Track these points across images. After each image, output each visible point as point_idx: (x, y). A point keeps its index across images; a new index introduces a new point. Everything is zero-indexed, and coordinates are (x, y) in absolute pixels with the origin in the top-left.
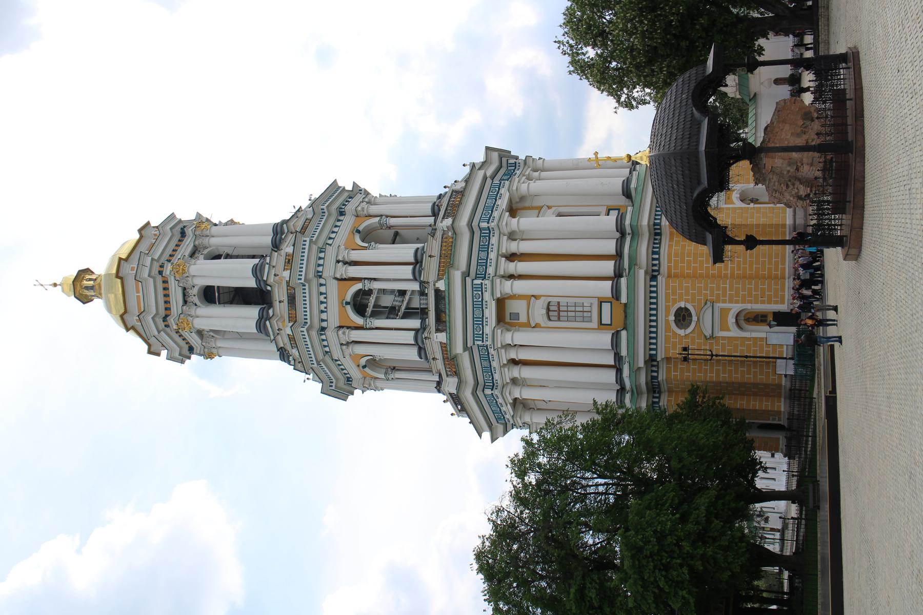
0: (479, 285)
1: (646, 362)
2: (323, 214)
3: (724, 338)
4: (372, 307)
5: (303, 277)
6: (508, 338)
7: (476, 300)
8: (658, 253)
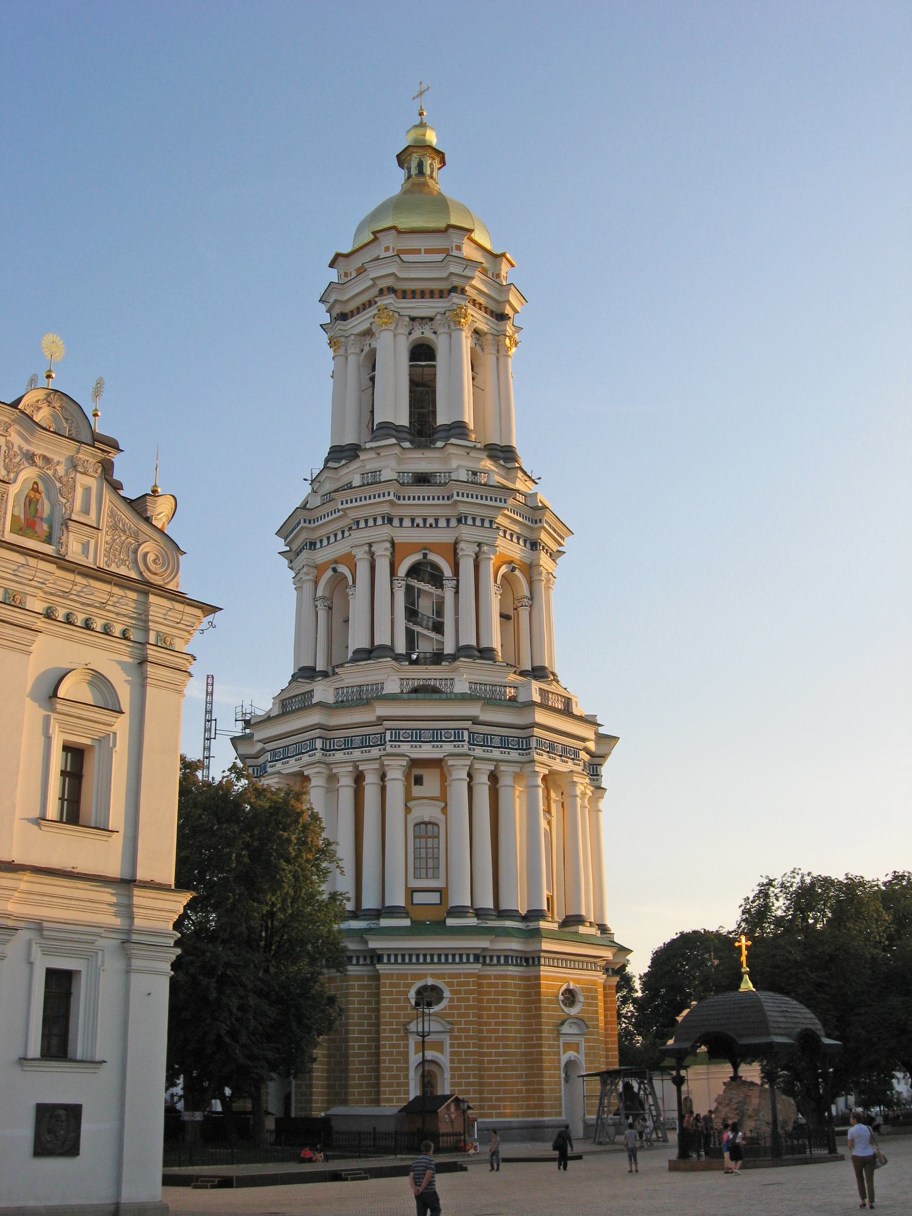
0: (462, 738)
1: (374, 950)
2: (534, 521)
3: (406, 1046)
4: (420, 586)
5: (460, 498)
6: (396, 775)
7: (443, 733)
8: (506, 963)
